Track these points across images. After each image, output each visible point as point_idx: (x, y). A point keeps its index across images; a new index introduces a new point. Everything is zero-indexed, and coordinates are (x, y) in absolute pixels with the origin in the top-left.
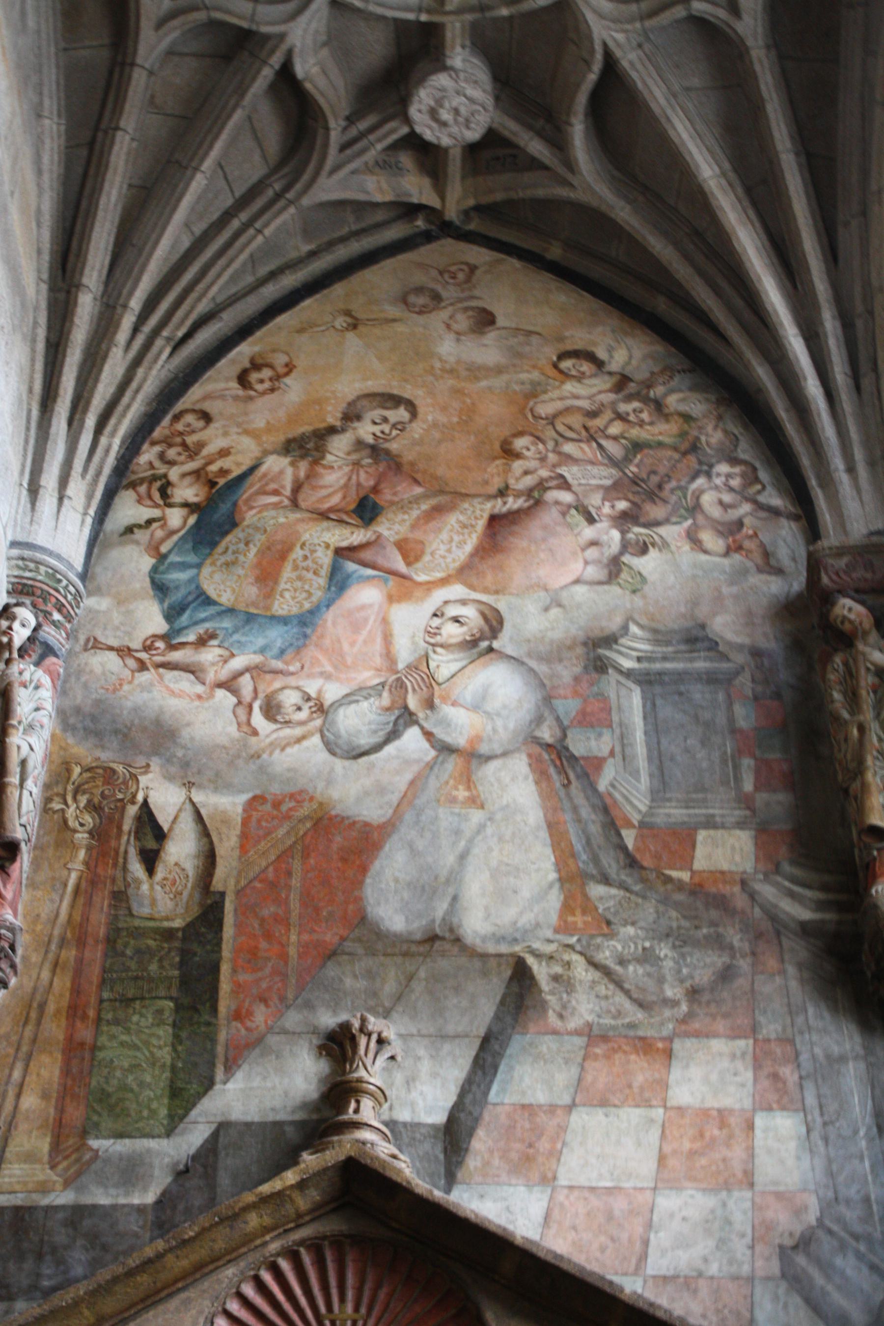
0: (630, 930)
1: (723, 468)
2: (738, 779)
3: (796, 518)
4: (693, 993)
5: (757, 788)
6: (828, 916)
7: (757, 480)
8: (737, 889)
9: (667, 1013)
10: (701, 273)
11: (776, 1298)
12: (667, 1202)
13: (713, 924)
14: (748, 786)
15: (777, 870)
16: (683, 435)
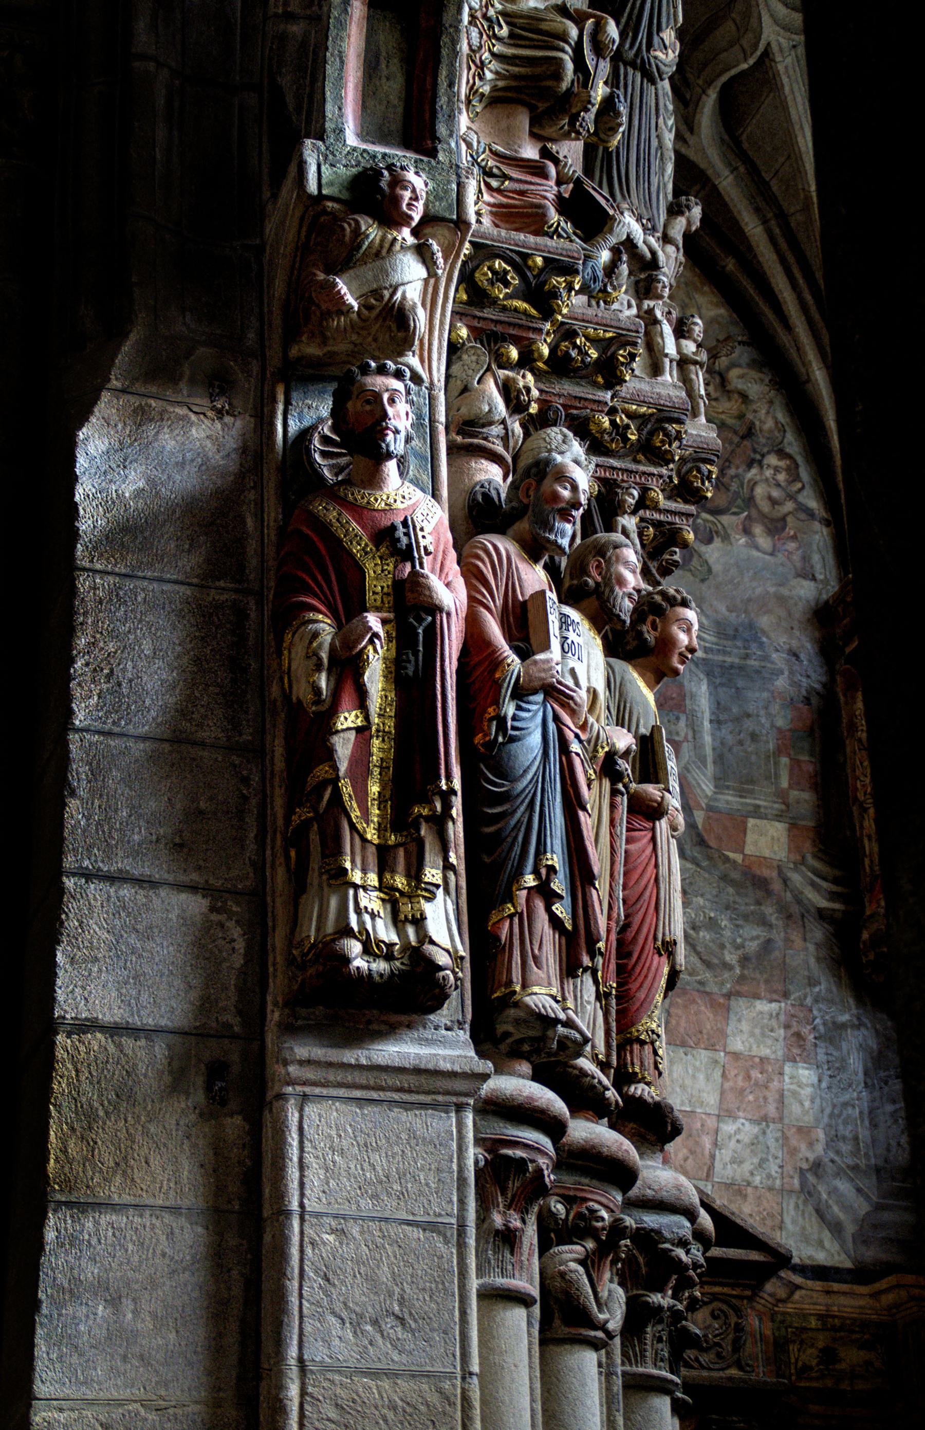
0: (701, 901)
1: (772, 460)
2: (777, 776)
3: (827, 523)
4: (744, 960)
5: (791, 787)
6: (837, 906)
7: (797, 478)
8: (775, 874)
9: (726, 975)
10: (783, 260)
11: (797, 1206)
12: (729, 1127)
13: (758, 903)
14: (785, 784)
15: (803, 861)
16: (741, 417)
